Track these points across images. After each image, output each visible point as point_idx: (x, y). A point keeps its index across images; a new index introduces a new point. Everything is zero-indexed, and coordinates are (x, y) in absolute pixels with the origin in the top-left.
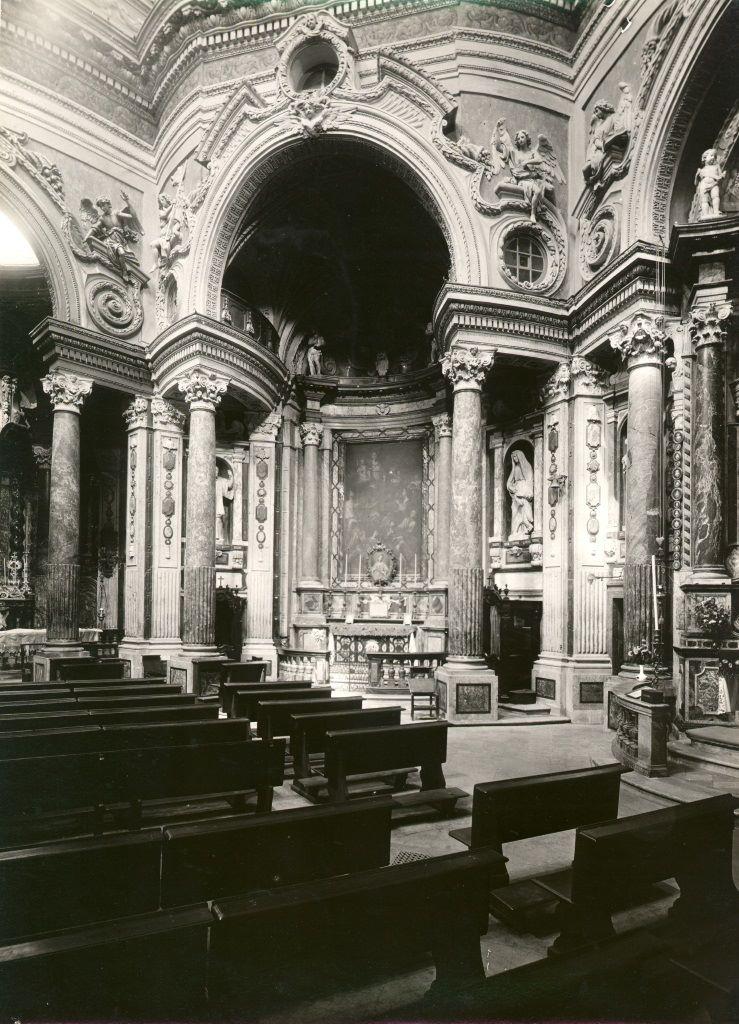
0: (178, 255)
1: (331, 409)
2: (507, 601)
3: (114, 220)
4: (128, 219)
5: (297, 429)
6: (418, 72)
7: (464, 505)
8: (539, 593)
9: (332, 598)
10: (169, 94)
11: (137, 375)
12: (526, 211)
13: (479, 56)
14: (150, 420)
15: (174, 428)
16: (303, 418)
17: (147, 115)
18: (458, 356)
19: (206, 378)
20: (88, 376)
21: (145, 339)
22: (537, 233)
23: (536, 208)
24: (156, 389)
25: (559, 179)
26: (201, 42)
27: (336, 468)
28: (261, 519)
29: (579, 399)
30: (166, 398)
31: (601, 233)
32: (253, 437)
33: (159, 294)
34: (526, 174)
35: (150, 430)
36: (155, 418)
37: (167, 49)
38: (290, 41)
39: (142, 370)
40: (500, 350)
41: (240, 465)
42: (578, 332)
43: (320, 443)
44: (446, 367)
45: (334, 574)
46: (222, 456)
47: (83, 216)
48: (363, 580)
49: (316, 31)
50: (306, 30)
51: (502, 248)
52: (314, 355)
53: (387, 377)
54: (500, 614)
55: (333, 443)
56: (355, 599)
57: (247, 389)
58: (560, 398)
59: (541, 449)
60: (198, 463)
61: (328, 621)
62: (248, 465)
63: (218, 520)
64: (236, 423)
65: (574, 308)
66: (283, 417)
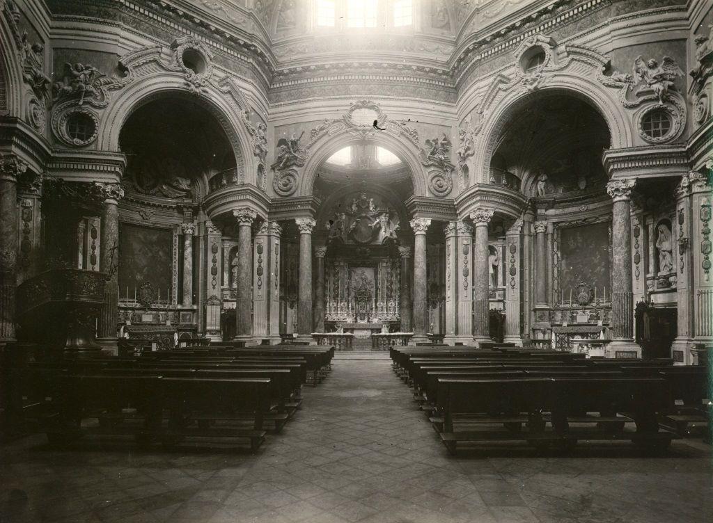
0: (468, 155)
1: (551, 212)
2: (653, 309)
3: (439, 145)
4: (446, 144)
5: (532, 225)
6: (583, 48)
7: (620, 260)
8: (675, 304)
9: (554, 313)
10: (463, 80)
11: (449, 212)
12: (657, 99)
13: (624, 28)
14: (456, 232)
15: (468, 234)
16: (535, 219)
17: (453, 90)
18: (614, 185)
19: (482, 211)
20: (429, 217)
21: (454, 195)
22: (665, 109)
23: (662, 97)
24: (459, 217)
25: (680, 75)
27: (556, 243)
28: (513, 273)
29: (694, 195)
30: (464, 221)
31: (702, 105)
32: (508, 233)
33: (460, 172)
34: (654, 81)
35: (457, 237)
36: (459, 231)
37: (462, 63)
38: (520, 50)
39: (452, 210)
40: (640, 177)
41: (501, 248)
42: (693, 158)
43: (546, 231)
44: (609, 190)
45: (555, 298)
46: (491, 244)
47: (427, 147)
48: (573, 303)
49: (534, 44)
51: (641, 124)
52: (541, 185)
53: (585, 190)
54: (649, 316)
55: (554, 230)
56: (568, 314)
57: (502, 211)
58: (684, 195)
59: (676, 226)
60: (480, 251)
61: (552, 326)
62: (505, 247)
63: (490, 276)
64: (498, 227)
65: (688, 147)
66: (524, 221)
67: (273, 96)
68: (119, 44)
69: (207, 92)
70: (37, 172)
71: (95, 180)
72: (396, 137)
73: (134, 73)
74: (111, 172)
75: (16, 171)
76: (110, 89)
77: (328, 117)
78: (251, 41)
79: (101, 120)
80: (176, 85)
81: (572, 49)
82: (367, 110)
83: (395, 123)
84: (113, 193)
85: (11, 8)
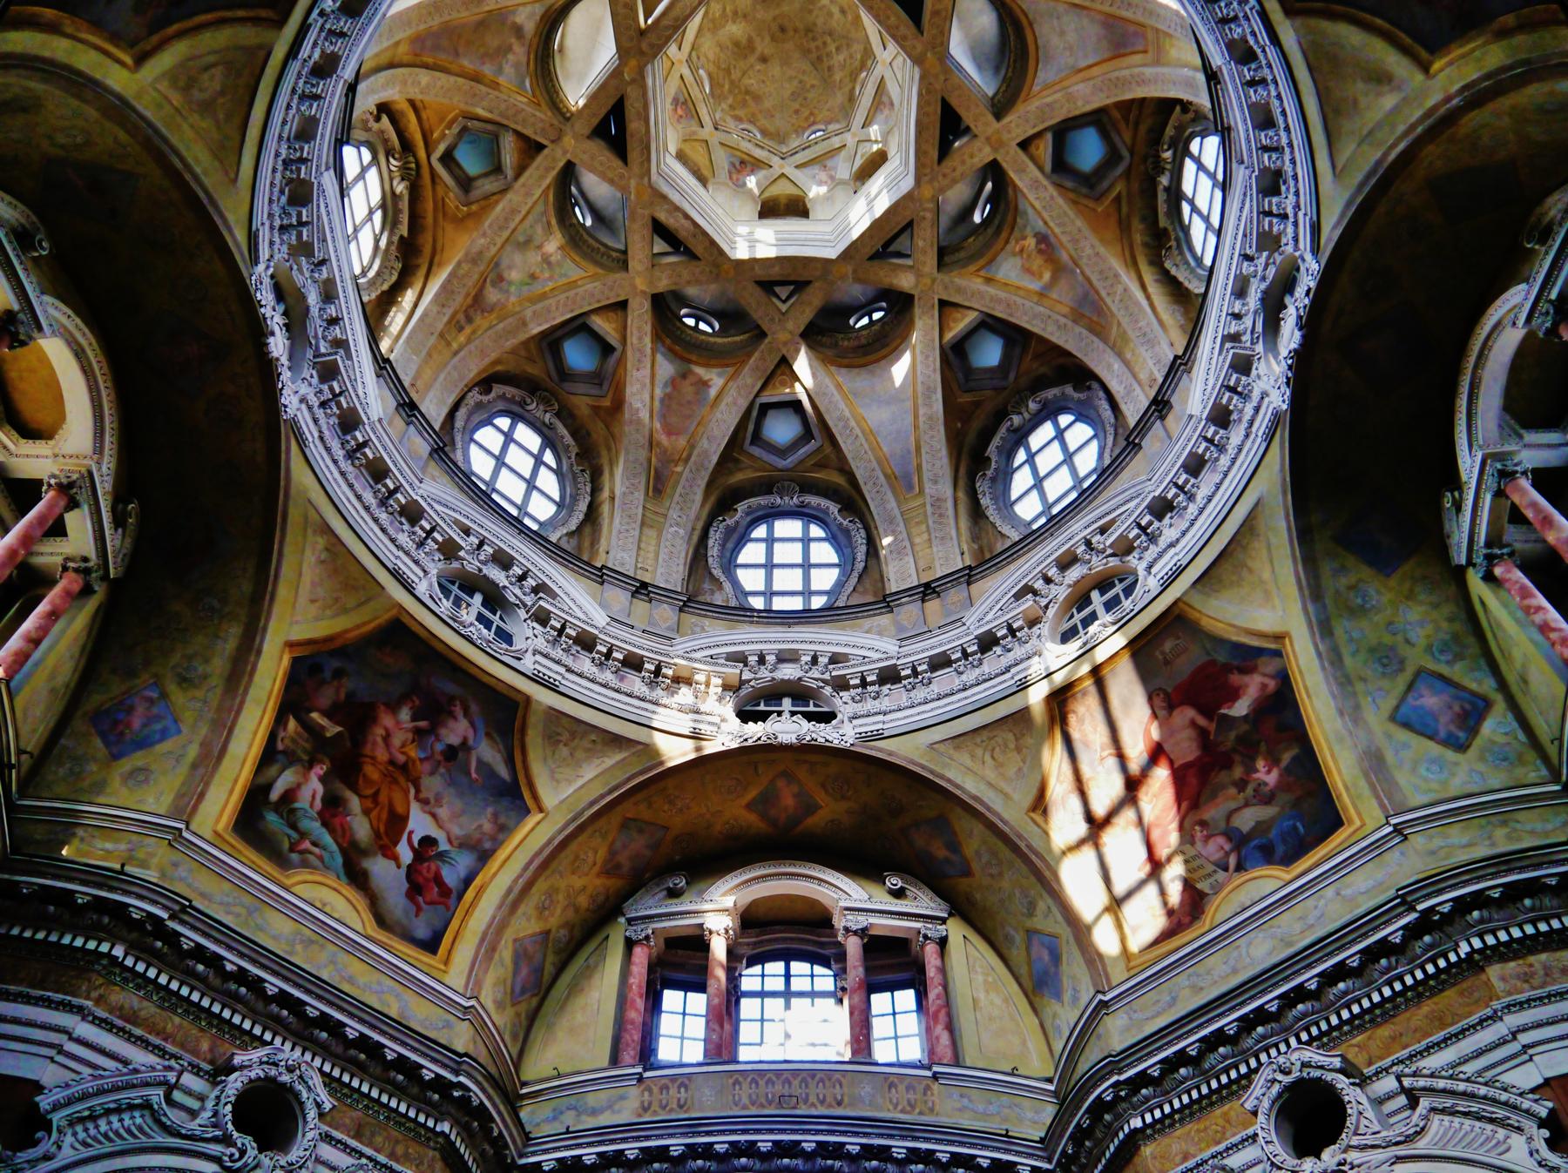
26: (1136, 1123)
38: (1261, 1094)
49: (1296, 1074)
50: (1280, 1077)
68: (59, 1058)
73: (69, 1139)
81: (1422, 1083)
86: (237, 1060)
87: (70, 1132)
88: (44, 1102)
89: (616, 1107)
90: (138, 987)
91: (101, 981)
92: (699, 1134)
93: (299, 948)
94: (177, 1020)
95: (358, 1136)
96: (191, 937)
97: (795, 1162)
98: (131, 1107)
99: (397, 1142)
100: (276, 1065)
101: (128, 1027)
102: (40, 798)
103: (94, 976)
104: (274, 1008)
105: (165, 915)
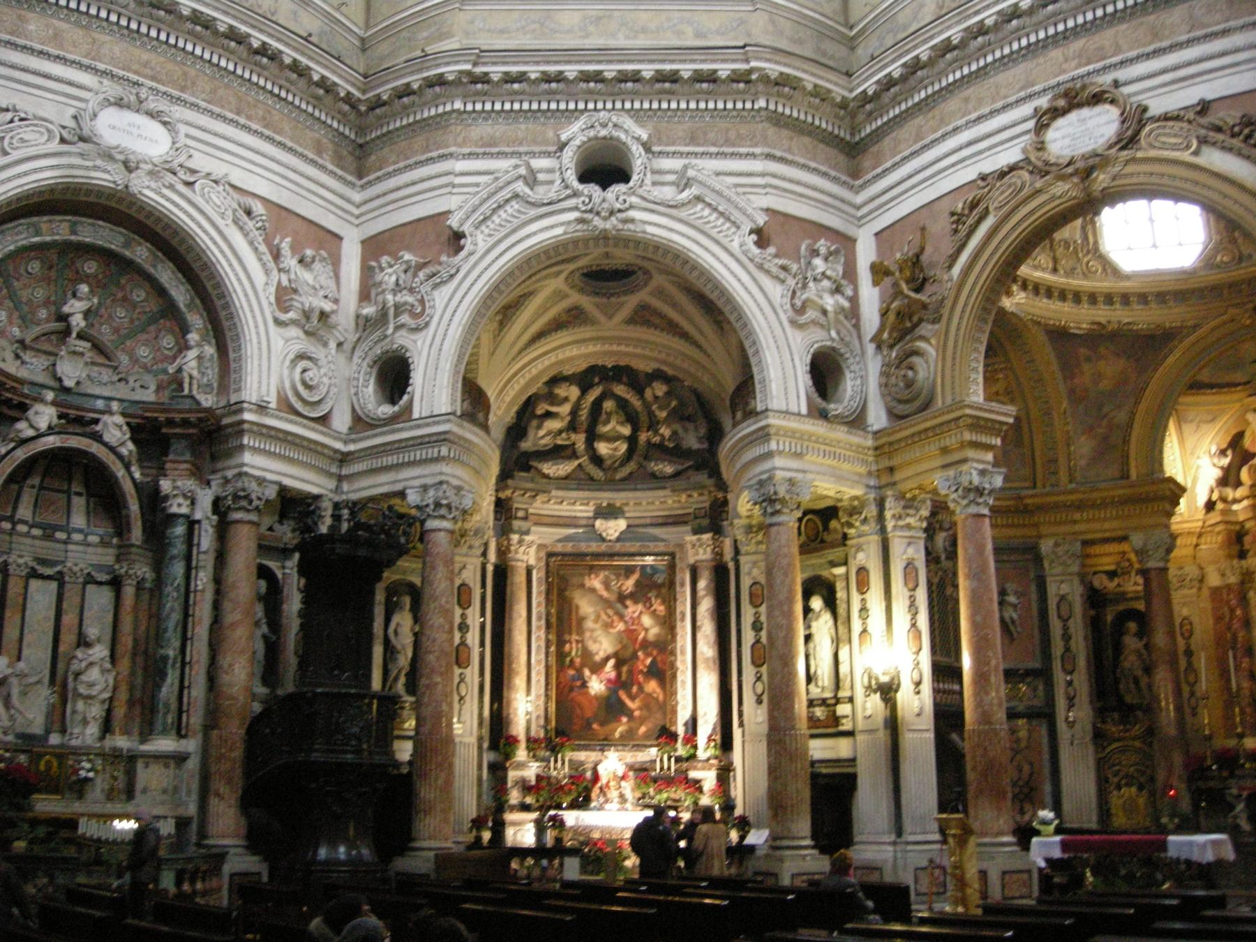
67: (867, 164)
68: (455, 190)
69: (632, 221)
70: (315, 490)
71: (407, 483)
72: (1186, 156)
73: (480, 237)
74: (437, 460)
75: (251, 502)
76: (436, 286)
77: (990, 164)
78: (747, 61)
79: (420, 354)
80: (559, 231)
82: (1085, 112)
83: (1177, 118)
84: (438, 505)
85: (249, 213)
86: (564, 137)
87: (478, 232)
88: (454, 222)
89: (920, 16)
90: (485, 119)
91: (459, 128)
92: (969, 17)
93: (592, 28)
94: (523, 127)
95: (693, 140)
96: (496, 71)
97: (1058, 5)
98: (507, 201)
99: (728, 130)
100: (592, 127)
101: (488, 150)
102: (376, 25)
103: (453, 128)
104: (583, 85)
105: (468, 67)
